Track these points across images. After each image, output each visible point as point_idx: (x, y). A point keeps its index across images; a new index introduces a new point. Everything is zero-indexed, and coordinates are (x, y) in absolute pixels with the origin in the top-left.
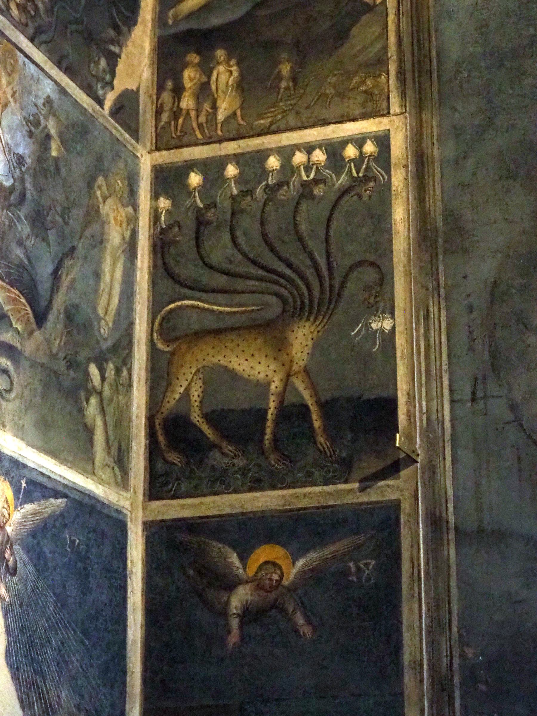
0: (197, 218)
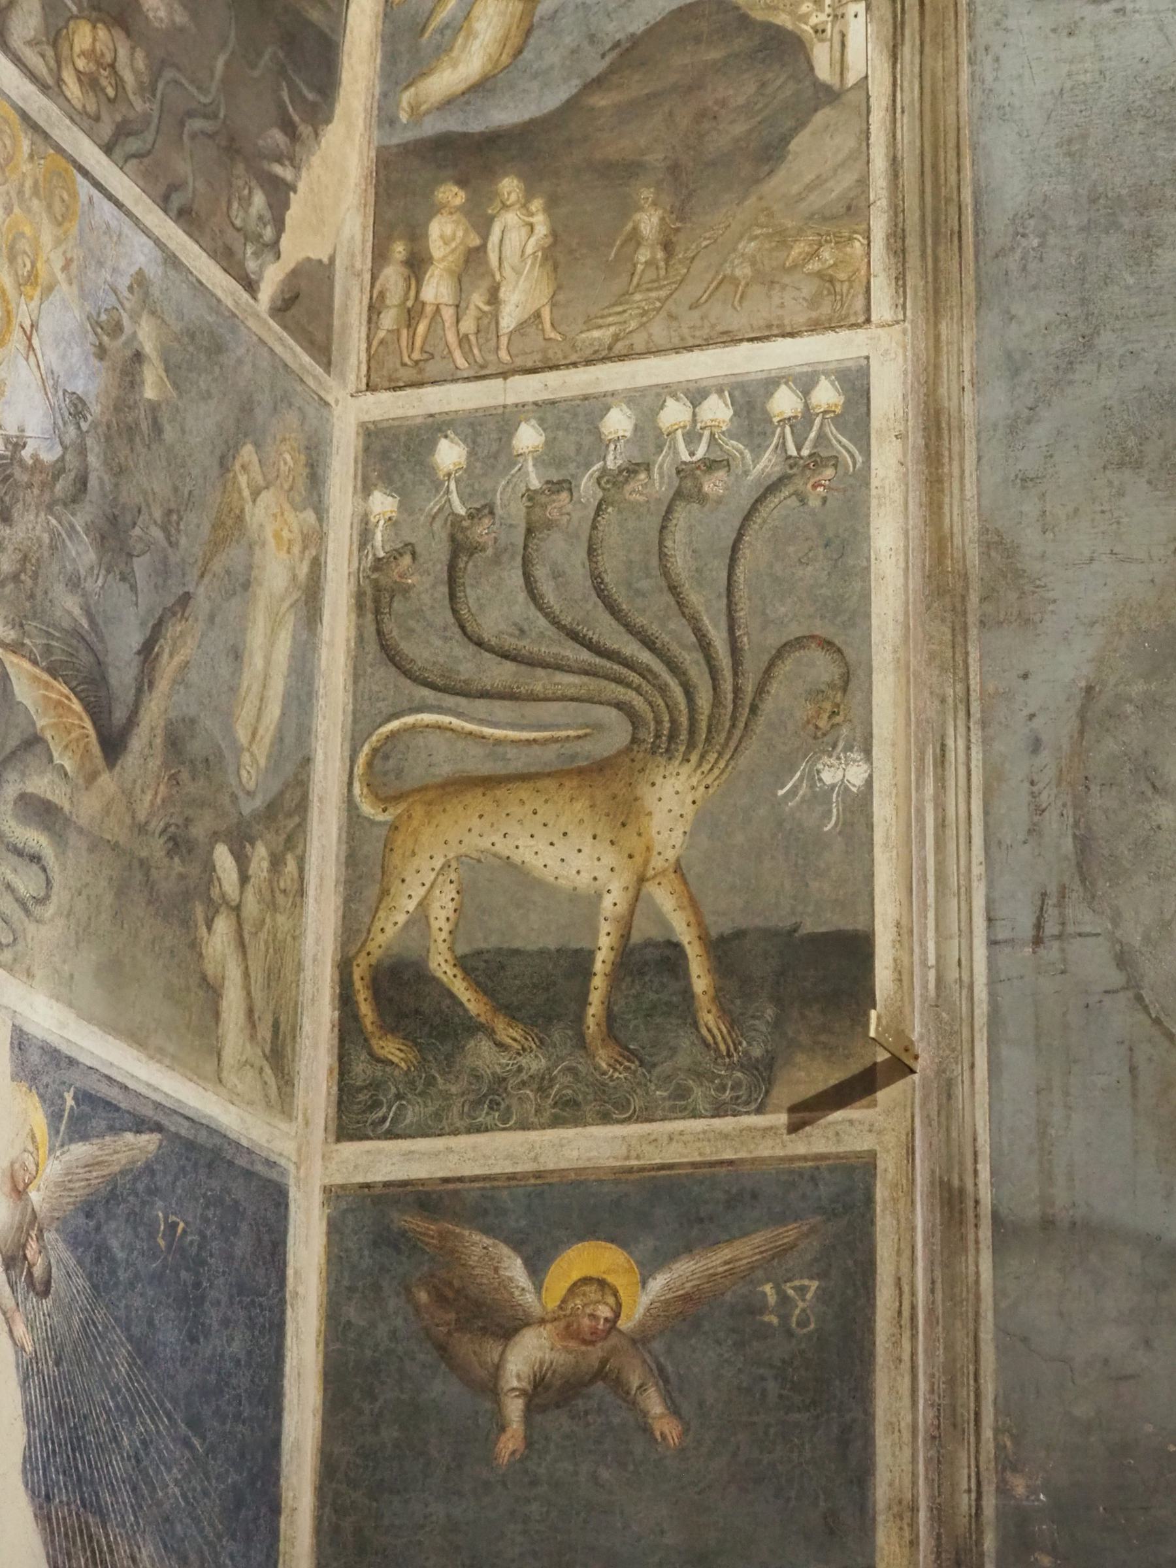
0: (453, 538)
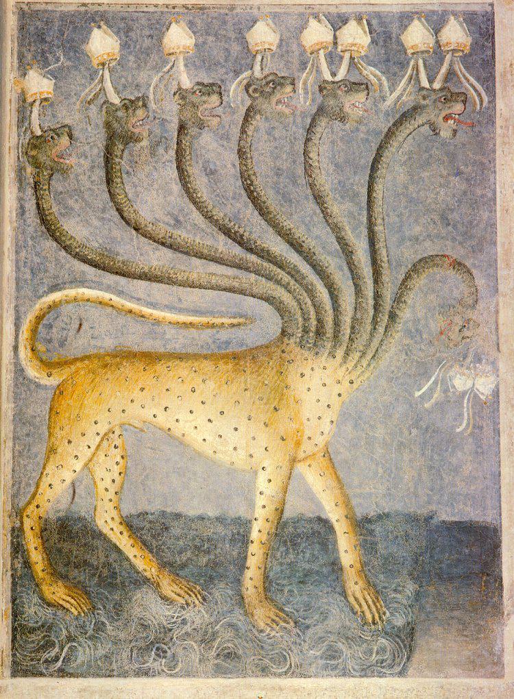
0: (108, 125)
